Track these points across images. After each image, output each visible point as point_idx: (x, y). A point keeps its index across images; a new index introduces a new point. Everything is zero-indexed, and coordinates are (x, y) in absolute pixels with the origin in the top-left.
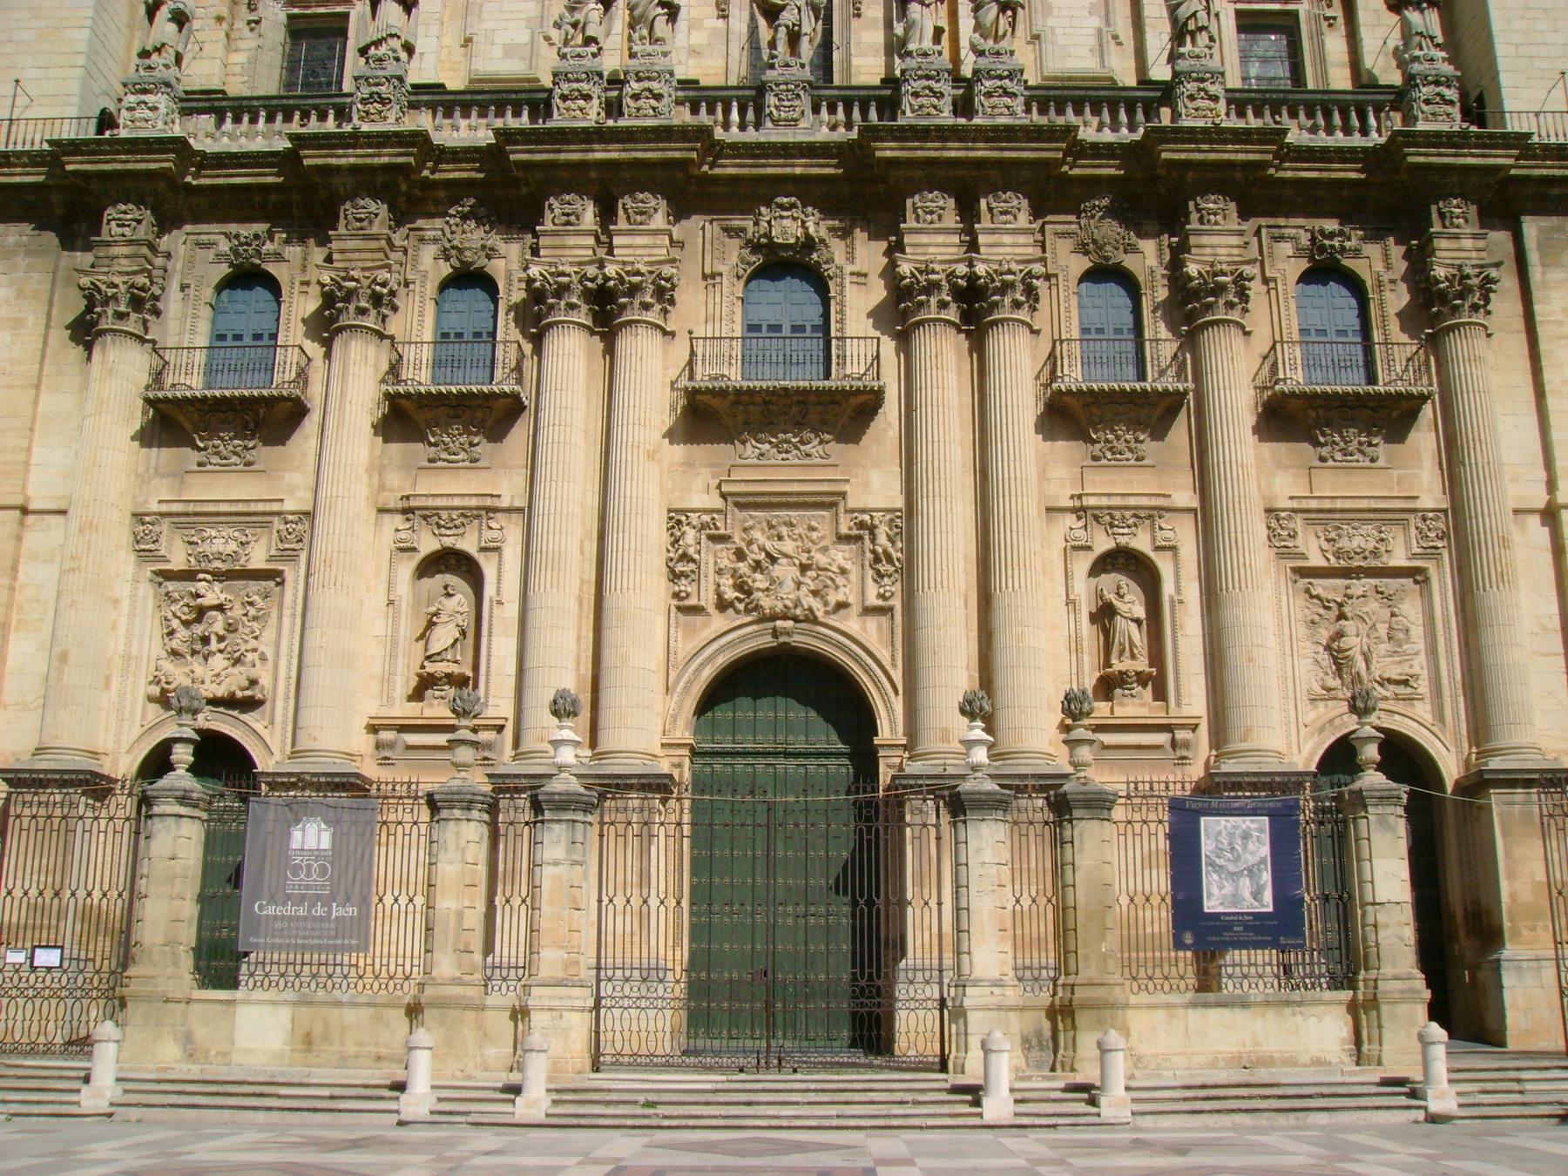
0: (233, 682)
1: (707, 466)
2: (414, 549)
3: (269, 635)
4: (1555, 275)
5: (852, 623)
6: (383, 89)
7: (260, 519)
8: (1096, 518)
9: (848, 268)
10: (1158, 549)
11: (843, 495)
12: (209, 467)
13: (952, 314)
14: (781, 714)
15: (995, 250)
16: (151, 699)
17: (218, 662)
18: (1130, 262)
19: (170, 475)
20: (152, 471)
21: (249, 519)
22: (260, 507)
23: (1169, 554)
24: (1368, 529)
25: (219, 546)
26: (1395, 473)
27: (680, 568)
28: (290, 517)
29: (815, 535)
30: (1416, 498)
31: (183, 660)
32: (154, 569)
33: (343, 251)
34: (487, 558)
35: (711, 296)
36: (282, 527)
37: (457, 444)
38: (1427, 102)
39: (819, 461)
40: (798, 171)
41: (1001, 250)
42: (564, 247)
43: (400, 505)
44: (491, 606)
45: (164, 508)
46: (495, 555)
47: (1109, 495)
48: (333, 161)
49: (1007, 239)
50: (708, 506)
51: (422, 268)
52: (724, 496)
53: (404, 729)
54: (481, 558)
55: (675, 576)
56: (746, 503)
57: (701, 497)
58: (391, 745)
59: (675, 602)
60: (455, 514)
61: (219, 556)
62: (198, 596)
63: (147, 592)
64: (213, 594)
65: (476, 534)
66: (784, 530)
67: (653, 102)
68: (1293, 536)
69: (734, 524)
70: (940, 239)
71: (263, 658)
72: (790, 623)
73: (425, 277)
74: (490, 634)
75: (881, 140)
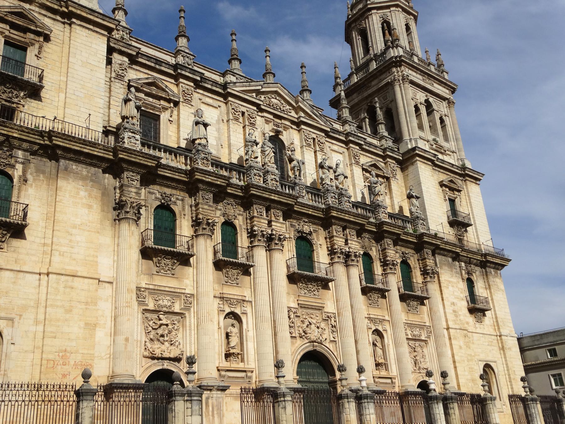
1: (293, 294)
2: (224, 311)
3: (180, 335)
4: (442, 271)
6: (207, 156)
7: (177, 294)
8: (372, 320)
10: (384, 330)
11: (324, 307)
12: (160, 274)
13: (342, 260)
14: (307, 370)
16: (145, 357)
18: (370, 252)
19: (148, 274)
20: (140, 272)
21: (174, 294)
22: (178, 291)
24: (418, 329)
26: (422, 316)
28: (189, 296)
31: (153, 343)
32: (144, 308)
33: (203, 208)
34: (243, 316)
35: (289, 244)
36: (185, 298)
37: (167, 268)
38: (421, 224)
39: (317, 297)
40: (310, 213)
43: (219, 296)
44: (246, 331)
45: (147, 286)
46: (245, 315)
47: (375, 315)
48: (204, 179)
50: (295, 307)
52: (298, 304)
53: (228, 371)
54: (241, 316)
55: (290, 327)
56: (301, 306)
57: (294, 305)
58: (224, 376)
60: (235, 301)
61: (165, 306)
62: (160, 320)
65: (240, 308)
69: (300, 312)
70: (341, 240)
72: (317, 344)
74: (247, 341)
75: (334, 210)
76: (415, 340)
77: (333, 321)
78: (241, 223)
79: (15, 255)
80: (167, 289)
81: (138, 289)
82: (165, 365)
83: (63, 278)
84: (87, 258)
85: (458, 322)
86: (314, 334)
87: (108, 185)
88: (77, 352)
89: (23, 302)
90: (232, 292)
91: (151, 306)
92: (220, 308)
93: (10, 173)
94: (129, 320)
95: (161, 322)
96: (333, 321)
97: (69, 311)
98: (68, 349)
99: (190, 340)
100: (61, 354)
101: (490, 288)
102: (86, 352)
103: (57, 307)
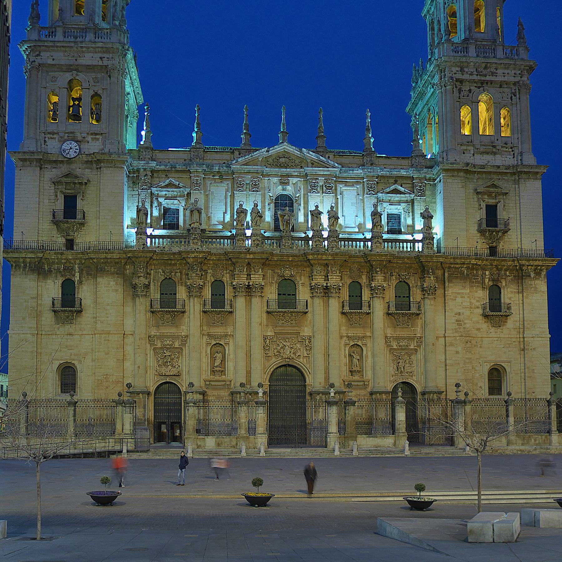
0: (174, 371)
5: (301, 360)
9: (300, 282)
15: (332, 280)
17: (170, 367)
21: (174, 337)
22: (177, 334)
23: (365, 345)
25: (168, 342)
27: (265, 348)
28: (184, 336)
29: (293, 341)
30: (416, 334)
41: (333, 280)
42: (240, 277)
45: (155, 334)
49: (334, 277)
51: (208, 279)
57: (270, 333)
59: (265, 355)
61: (168, 344)
63: (152, 352)
64: (168, 354)
66: (287, 340)
67: (258, 242)
68: (390, 342)
70: (320, 277)
71: (179, 366)
72: (289, 360)
73: (209, 282)
76: (402, 349)
77: (307, 342)
78: (228, 280)
79: (79, 326)
80: (168, 334)
81: (149, 337)
82: (168, 379)
83: (103, 336)
84: (116, 322)
85: (462, 330)
86: (287, 352)
87: (129, 274)
88: (113, 375)
89: (86, 350)
90: (218, 331)
91: (159, 345)
92: (208, 342)
93: (73, 279)
94: (140, 356)
95: (165, 354)
96: (307, 342)
97: (107, 354)
98: (108, 374)
99: (186, 364)
100: (104, 377)
101: (522, 292)
102: (118, 375)
103: (101, 351)
